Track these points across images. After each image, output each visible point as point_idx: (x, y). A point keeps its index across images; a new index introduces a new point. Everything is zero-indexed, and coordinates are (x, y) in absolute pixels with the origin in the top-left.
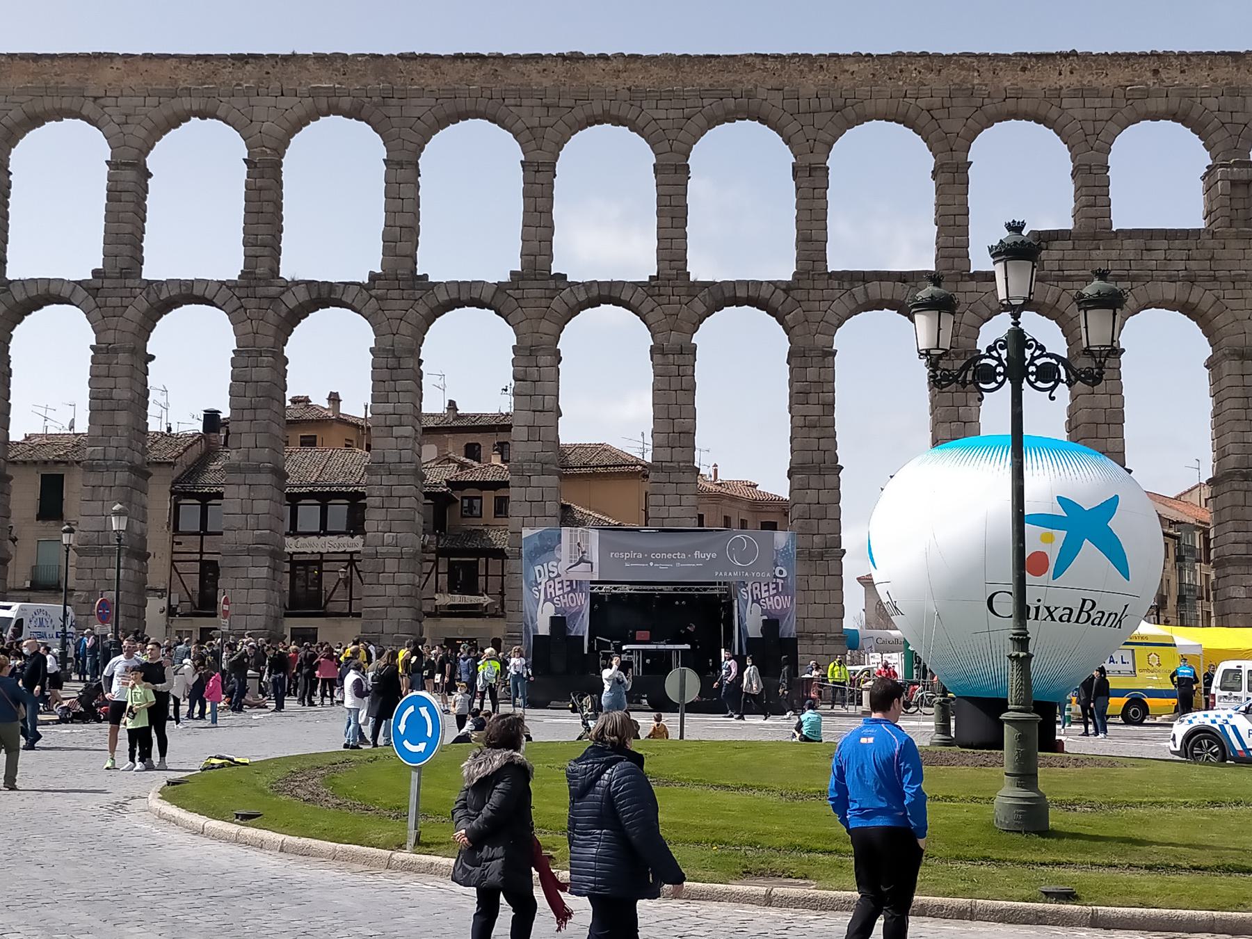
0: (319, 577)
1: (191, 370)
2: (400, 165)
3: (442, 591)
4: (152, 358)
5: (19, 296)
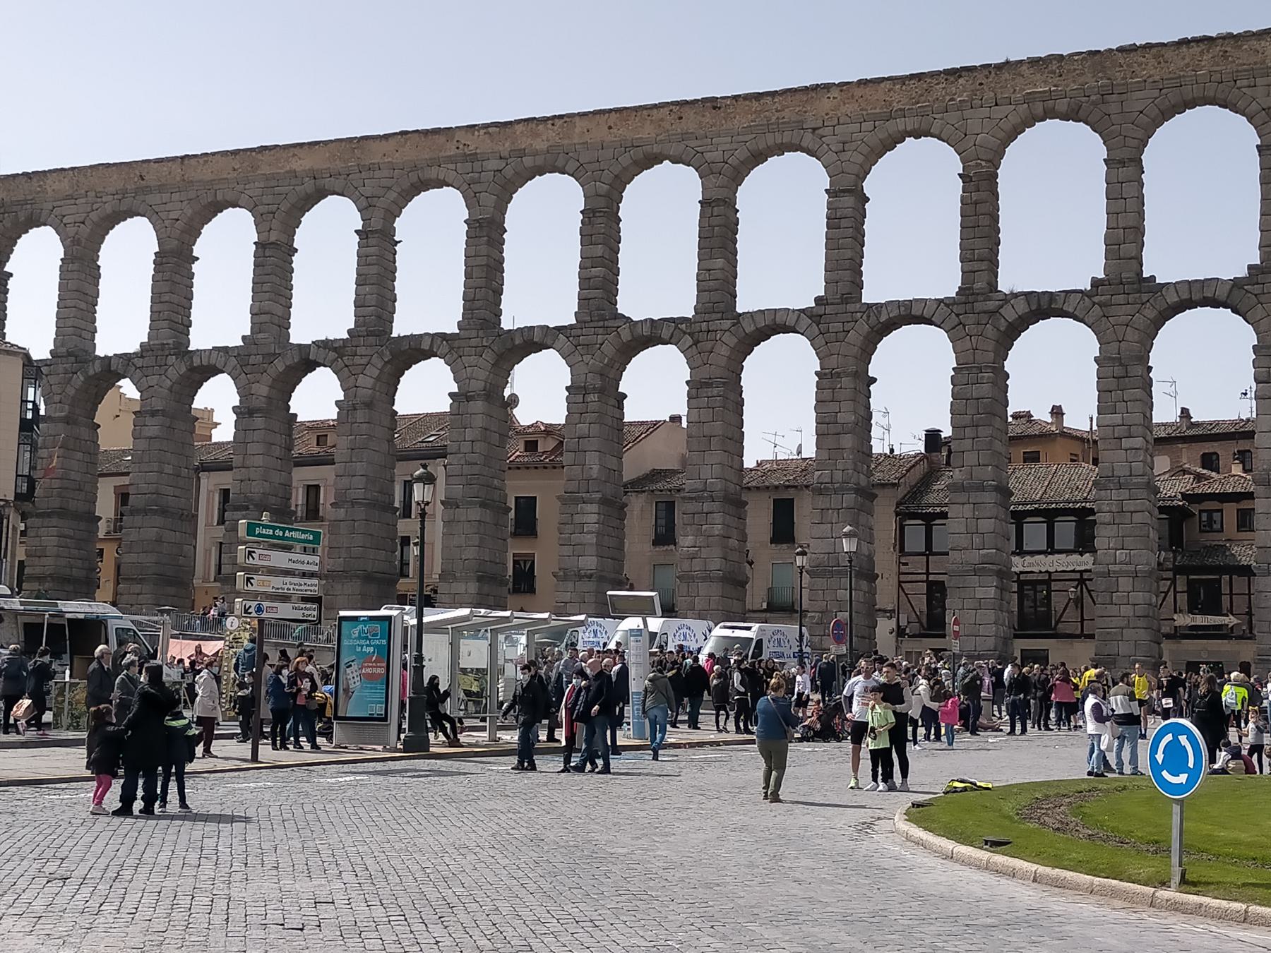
0: (1048, 597)
1: (912, 392)
2: (1122, 163)
3: (1181, 611)
4: (874, 380)
5: (749, 328)
